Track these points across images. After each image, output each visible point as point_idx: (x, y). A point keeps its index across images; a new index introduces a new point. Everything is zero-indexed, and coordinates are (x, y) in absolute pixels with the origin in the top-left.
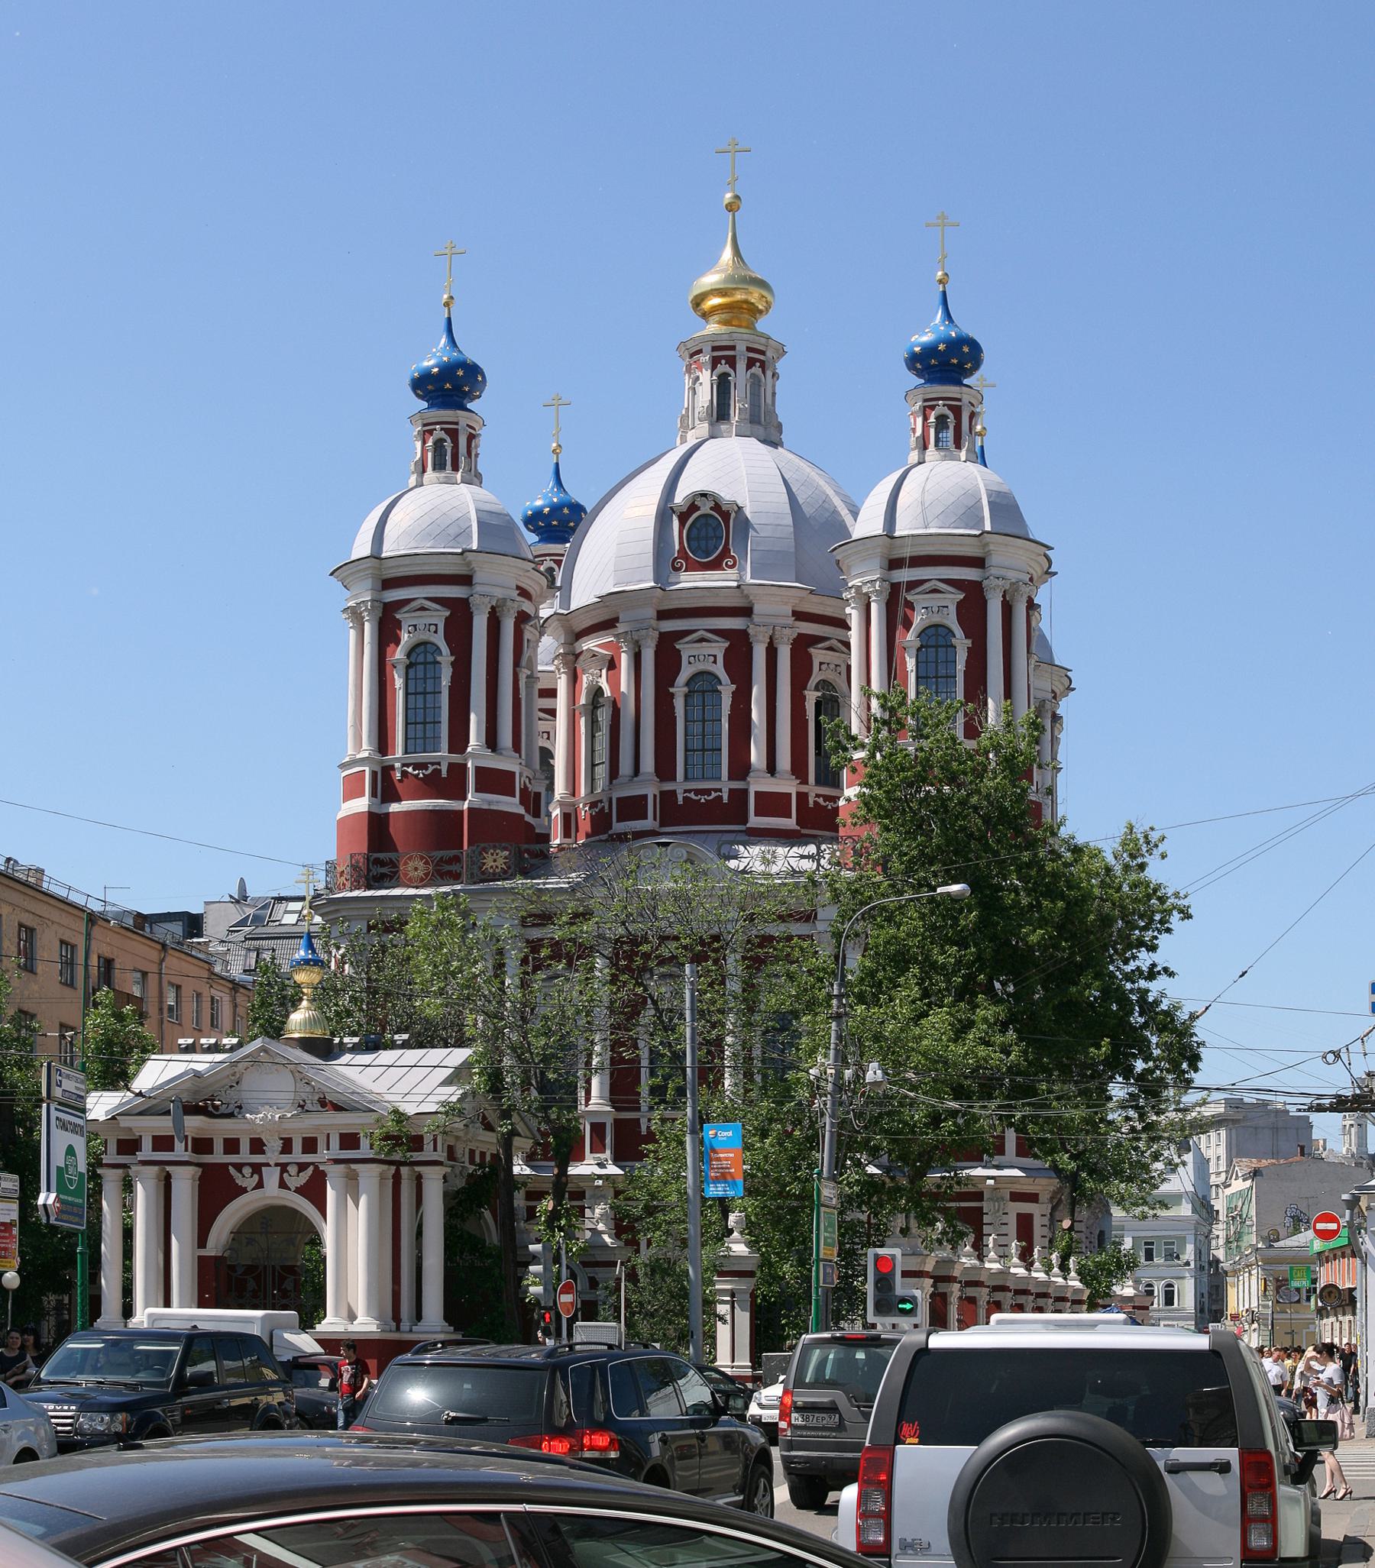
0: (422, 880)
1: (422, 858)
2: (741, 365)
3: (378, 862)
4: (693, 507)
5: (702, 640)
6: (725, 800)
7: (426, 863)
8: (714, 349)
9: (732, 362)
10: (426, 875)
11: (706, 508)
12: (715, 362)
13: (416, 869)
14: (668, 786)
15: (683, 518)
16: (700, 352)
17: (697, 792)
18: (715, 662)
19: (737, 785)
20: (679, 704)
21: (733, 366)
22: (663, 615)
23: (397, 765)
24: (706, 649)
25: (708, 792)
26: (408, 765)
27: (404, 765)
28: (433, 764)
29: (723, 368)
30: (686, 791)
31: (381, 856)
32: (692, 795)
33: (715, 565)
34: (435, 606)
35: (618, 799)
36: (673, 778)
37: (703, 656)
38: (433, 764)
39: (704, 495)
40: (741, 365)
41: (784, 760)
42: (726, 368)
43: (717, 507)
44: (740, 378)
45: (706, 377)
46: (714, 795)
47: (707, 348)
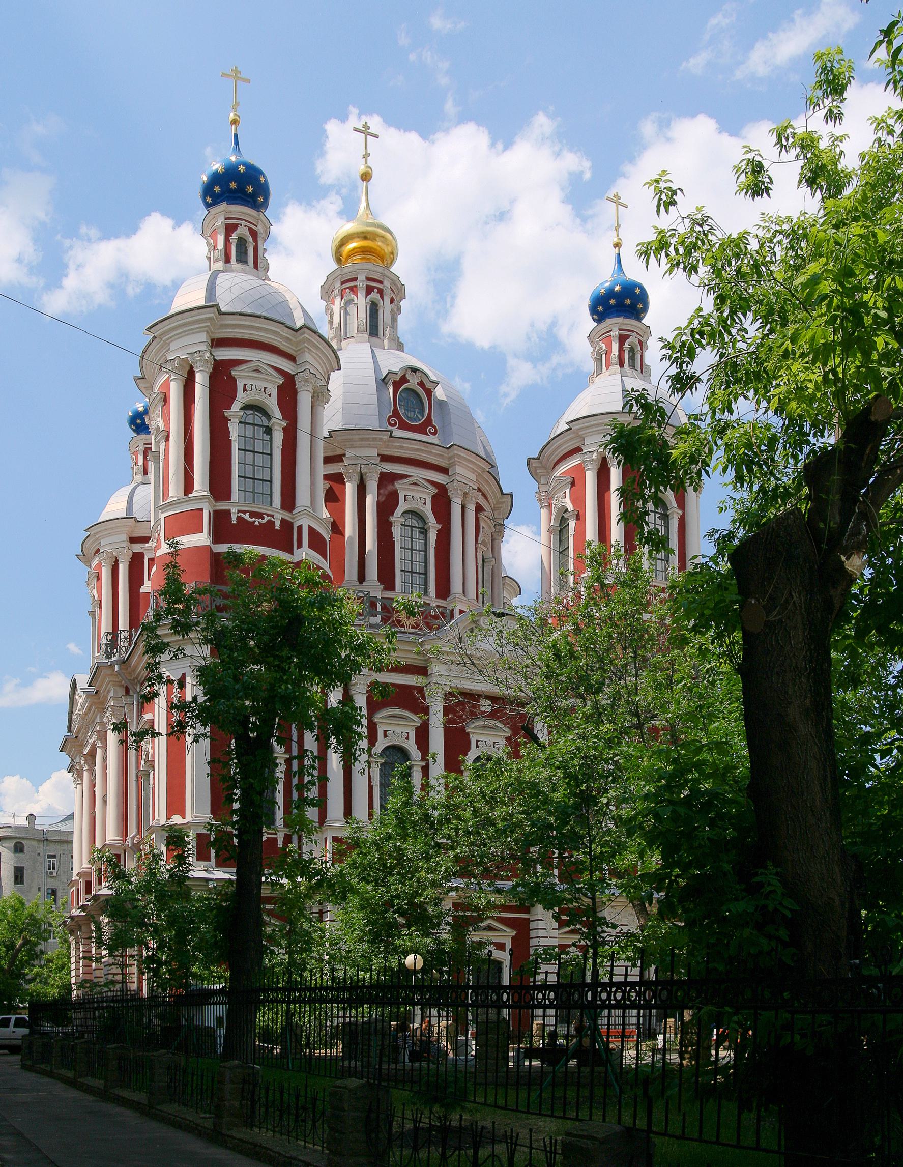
2: (387, 299)
4: (404, 380)
9: (381, 292)
12: (369, 290)
15: (397, 385)
16: (355, 279)
21: (382, 297)
22: (384, 458)
23: (234, 510)
26: (244, 512)
27: (239, 511)
28: (268, 515)
29: (375, 295)
33: (421, 429)
37: (415, 496)
38: (268, 515)
40: (387, 299)
42: (378, 296)
43: (421, 384)
44: (386, 308)
45: (361, 301)
47: (362, 278)
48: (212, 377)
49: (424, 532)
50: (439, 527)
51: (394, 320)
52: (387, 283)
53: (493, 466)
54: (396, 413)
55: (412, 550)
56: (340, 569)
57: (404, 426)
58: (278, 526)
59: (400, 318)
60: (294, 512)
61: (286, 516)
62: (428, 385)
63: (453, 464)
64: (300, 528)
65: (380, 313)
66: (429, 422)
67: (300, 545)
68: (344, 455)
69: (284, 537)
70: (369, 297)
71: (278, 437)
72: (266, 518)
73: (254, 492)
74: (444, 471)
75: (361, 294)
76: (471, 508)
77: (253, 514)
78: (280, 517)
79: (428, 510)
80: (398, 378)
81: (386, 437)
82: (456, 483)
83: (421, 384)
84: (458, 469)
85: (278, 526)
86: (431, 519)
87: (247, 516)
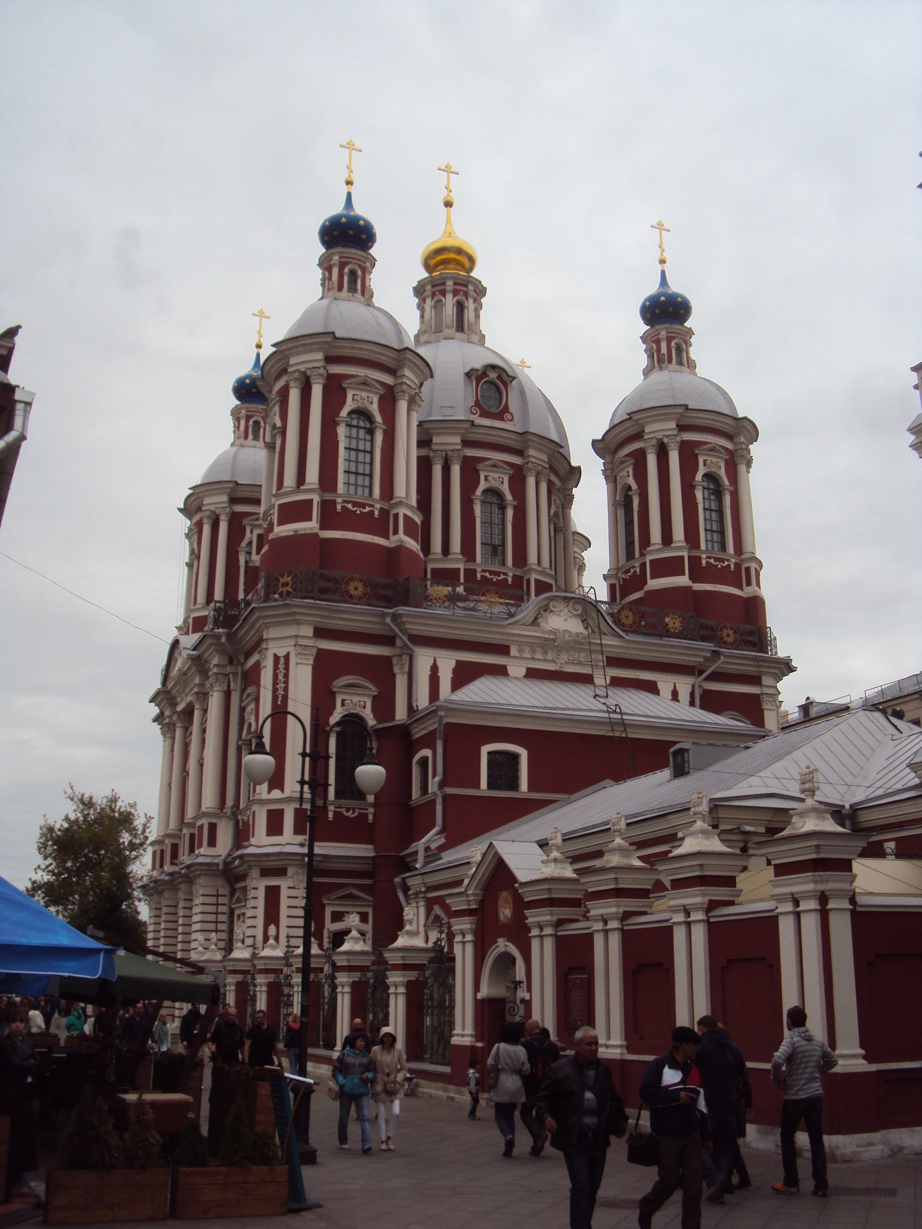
0: (360, 598)
1: (361, 581)
2: (471, 301)
3: (322, 577)
5: (494, 466)
6: (510, 580)
7: (365, 585)
8: (455, 284)
9: (466, 294)
10: (365, 594)
11: (493, 375)
12: (455, 293)
13: (356, 589)
14: (471, 566)
15: (478, 380)
17: (491, 573)
18: (502, 483)
19: (519, 572)
20: (477, 508)
21: (467, 299)
22: (466, 443)
23: (339, 500)
24: (494, 475)
25: (498, 574)
26: (348, 502)
27: (344, 502)
30: (483, 571)
31: (326, 572)
32: (487, 574)
33: (500, 416)
34: (376, 384)
35: (433, 570)
36: (473, 559)
39: (494, 367)
40: (471, 301)
41: (546, 562)
42: (464, 298)
44: (470, 305)
45: (450, 302)
46: (502, 577)
47: (450, 283)
48: (325, 388)
49: (502, 508)
50: (515, 503)
51: (478, 316)
52: (471, 287)
53: (562, 447)
54: (477, 404)
55: (491, 524)
56: (426, 547)
57: (485, 414)
58: (376, 513)
59: (482, 313)
60: (392, 502)
61: (386, 506)
62: (505, 377)
63: (528, 447)
64: (396, 516)
65: (466, 311)
66: (506, 409)
67: (396, 532)
68: (431, 440)
69: (381, 524)
70: (455, 299)
71: (379, 437)
72: (367, 509)
73: (356, 485)
74: (520, 453)
75: (449, 296)
76: (544, 486)
77: (355, 504)
78: (378, 506)
79: (505, 488)
80: (480, 373)
81: (467, 425)
82: (530, 465)
83: (499, 378)
84: (532, 452)
85: (376, 513)
86: (509, 497)
87: (350, 506)
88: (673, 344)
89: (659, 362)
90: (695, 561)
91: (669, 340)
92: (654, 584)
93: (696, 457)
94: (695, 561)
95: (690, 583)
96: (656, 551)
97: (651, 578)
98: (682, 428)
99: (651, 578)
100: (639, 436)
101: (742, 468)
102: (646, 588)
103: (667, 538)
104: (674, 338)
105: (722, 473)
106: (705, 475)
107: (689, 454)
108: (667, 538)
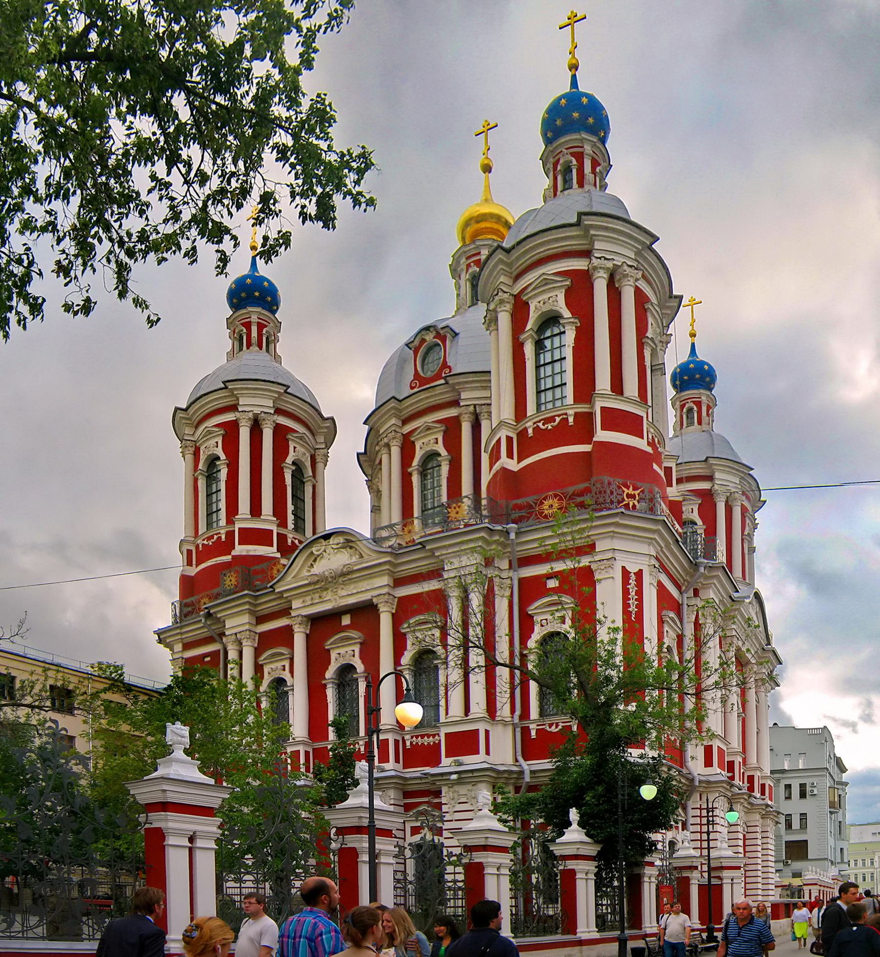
88: (264, 332)
89: (249, 345)
90: (282, 538)
91: (261, 327)
92: (240, 550)
93: (287, 441)
94: (282, 538)
95: (278, 555)
96: (244, 520)
97: (239, 544)
98: (278, 411)
99: (239, 544)
100: (234, 408)
101: (320, 466)
102: (234, 553)
103: (256, 510)
104: (266, 326)
105: (308, 464)
106: (294, 463)
107: (281, 435)
108: (256, 510)
